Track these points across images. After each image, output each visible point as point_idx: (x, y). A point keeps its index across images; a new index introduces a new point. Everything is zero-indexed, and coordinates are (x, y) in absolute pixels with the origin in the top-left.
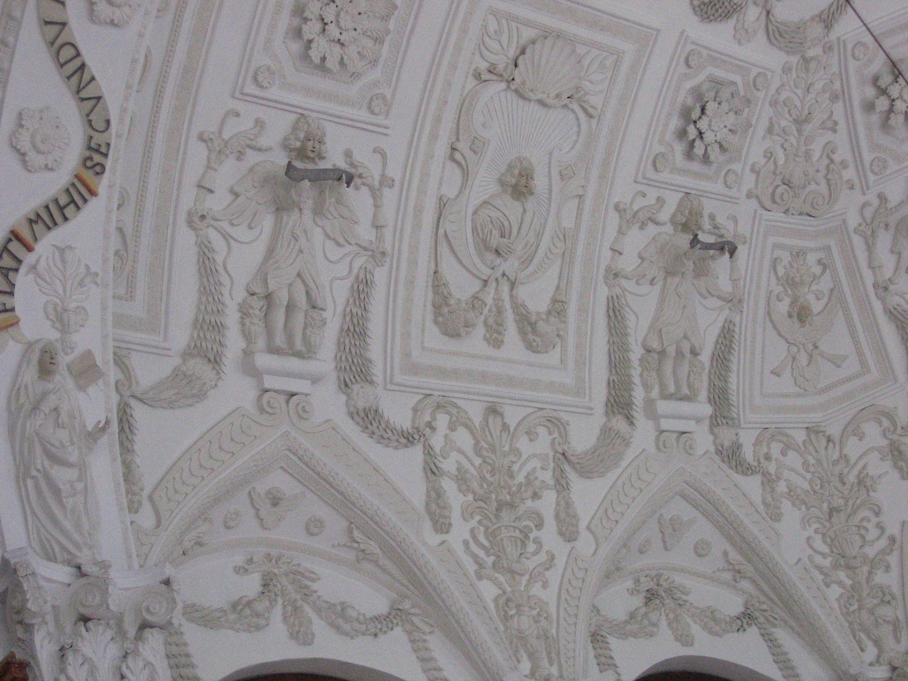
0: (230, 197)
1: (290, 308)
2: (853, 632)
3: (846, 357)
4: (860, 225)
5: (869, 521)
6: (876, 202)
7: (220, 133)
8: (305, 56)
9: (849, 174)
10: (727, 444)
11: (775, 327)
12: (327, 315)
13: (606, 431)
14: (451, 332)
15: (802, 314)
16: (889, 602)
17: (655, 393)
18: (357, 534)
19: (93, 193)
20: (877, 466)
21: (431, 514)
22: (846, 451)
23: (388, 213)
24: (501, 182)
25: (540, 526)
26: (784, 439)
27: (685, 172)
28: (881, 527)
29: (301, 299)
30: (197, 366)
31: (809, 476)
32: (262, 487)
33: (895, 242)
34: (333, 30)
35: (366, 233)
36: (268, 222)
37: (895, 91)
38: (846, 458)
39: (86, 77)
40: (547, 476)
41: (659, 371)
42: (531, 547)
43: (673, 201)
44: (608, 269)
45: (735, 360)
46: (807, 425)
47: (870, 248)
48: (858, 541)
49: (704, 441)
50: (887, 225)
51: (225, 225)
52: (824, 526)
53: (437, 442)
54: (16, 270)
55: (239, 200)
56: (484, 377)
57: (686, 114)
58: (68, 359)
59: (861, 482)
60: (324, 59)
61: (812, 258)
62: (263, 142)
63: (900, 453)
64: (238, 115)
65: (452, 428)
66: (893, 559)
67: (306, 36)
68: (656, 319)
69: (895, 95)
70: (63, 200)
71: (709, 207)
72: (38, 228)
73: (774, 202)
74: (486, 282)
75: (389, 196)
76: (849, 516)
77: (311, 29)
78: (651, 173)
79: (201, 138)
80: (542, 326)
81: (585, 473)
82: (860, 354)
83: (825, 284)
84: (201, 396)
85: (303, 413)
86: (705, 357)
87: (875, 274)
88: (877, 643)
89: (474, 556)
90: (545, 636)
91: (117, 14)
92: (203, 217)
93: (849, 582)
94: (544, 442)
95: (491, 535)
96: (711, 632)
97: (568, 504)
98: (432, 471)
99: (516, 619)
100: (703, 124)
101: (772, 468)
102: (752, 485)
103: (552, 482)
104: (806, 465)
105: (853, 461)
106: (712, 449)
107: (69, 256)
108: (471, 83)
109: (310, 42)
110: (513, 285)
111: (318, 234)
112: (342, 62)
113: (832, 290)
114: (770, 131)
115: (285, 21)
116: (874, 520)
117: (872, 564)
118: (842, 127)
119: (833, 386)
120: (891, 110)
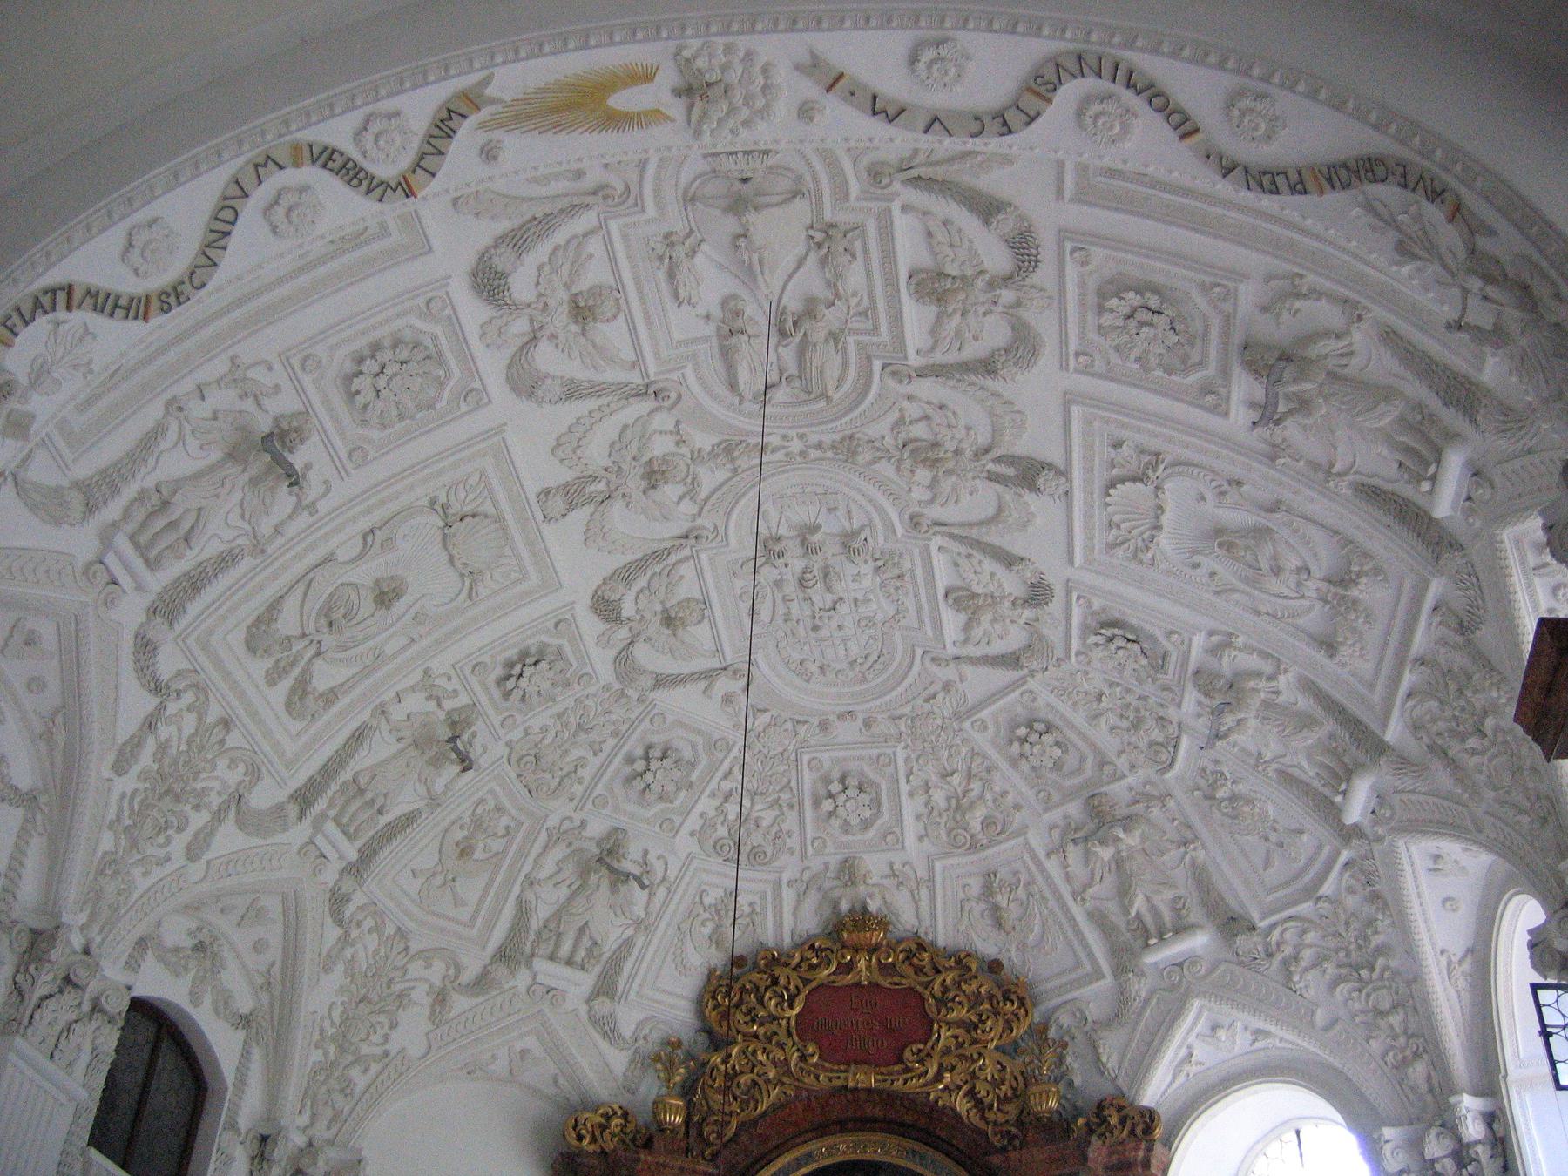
0: (209, 415)
1: (172, 525)
2: (306, 1093)
5: (382, 1027)
7: (249, 368)
8: (349, 378)
9: (578, 789)
10: (343, 890)
11: (441, 844)
12: (190, 554)
13: (280, 807)
14: (251, 646)
17: (332, 813)
18: (59, 720)
19: (145, 318)
20: (421, 995)
21: (121, 753)
23: (292, 529)
24: (377, 582)
25: (180, 830)
26: (379, 922)
27: (486, 689)
28: (386, 1038)
29: (185, 526)
30: (76, 500)
32: (31, 623)
33: (564, 859)
34: (382, 382)
35: (266, 528)
36: (216, 455)
37: (654, 765)
38: (406, 971)
39: (222, 243)
40: (215, 801)
41: (348, 802)
42: (161, 840)
43: (464, 699)
44: (382, 705)
45: (399, 840)
47: (546, 848)
48: (363, 1036)
49: (330, 875)
51: (188, 428)
53: (172, 708)
54: (46, 312)
55: (216, 424)
56: (242, 695)
57: (524, 654)
58: (18, 406)
59: (401, 995)
60: (358, 392)
61: (505, 821)
62: (266, 402)
63: (444, 999)
64: (270, 369)
65: (190, 709)
66: (375, 1068)
67: (364, 368)
68: (379, 765)
69: (653, 768)
70: (123, 302)
71: (479, 726)
72: (89, 301)
73: (518, 762)
74: (304, 635)
75: (304, 519)
77: (370, 366)
78: (467, 670)
79: (233, 359)
80: (310, 700)
81: (241, 824)
82: (478, 910)
83: (497, 845)
84: (58, 522)
85: (109, 602)
86: (384, 820)
88: (314, 1116)
89: (120, 809)
90: (115, 908)
91: (283, 227)
92: (180, 409)
93: (332, 1057)
94: (235, 776)
95: (145, 805)
96: (216, 1011)
97: (212, 834)
98: (150, 724)
99: (108, 878)
100: (528, 671)
101: (354, 934)
102: (333, 933)
103: (215, 808)
104: (376, 952)
105: (408, 977)
106: (331, 885)
107: (89, 338)
108: (425, 501)
109: (361, 373)
110: (318, 654)
111: (237, 496)
112: (365, 407)
113: (497, 853)
114: (560, 716)
115: (361, 344)
117: (358, 1060)
118: (602, 756)
120: (641, 775)
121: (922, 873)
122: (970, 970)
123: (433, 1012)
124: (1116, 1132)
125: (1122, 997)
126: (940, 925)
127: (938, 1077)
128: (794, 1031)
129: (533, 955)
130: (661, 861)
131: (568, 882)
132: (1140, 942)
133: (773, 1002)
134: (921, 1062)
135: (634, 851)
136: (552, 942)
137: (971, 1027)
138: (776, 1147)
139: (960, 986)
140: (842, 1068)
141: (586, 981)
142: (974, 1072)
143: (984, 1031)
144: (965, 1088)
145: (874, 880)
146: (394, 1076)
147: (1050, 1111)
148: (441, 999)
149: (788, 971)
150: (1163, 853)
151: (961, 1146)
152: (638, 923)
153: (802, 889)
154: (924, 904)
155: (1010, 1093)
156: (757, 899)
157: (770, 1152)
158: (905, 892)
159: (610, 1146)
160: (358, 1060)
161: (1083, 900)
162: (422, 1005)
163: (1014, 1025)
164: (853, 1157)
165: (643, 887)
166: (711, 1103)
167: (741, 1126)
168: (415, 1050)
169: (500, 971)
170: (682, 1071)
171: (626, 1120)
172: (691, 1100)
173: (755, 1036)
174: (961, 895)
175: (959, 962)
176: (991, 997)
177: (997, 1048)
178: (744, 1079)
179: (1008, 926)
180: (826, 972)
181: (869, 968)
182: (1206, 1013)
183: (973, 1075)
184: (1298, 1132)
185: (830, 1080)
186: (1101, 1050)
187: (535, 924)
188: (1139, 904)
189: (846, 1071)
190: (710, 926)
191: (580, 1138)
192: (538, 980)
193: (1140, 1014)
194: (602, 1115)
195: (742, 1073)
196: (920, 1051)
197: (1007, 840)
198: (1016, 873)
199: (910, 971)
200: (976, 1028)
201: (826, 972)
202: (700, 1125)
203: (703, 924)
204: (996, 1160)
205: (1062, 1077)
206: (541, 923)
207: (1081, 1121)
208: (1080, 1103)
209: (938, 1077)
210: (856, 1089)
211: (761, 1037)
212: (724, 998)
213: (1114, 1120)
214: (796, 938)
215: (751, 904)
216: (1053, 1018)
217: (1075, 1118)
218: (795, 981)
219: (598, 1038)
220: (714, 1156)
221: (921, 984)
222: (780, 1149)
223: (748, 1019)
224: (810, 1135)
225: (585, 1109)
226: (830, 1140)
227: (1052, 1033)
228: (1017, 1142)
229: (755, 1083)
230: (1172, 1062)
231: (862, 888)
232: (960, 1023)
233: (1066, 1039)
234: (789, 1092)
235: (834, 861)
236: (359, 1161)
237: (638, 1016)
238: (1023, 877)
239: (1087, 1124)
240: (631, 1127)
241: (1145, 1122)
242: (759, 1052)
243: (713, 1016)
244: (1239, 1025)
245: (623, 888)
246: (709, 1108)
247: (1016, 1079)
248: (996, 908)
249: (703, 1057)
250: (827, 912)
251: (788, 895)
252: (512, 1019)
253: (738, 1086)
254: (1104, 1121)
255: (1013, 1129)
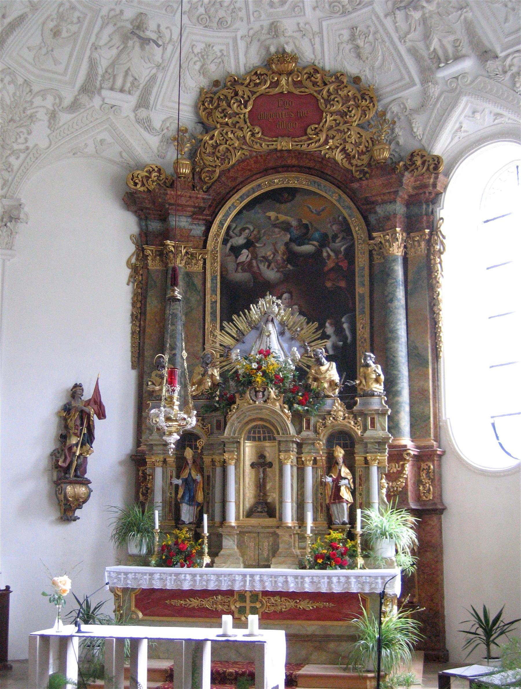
3: (60, 63)
4: (105, 16)
5: (23, 134)
6: (118, 12)
15: (56, 33)
16: (9, 172)
20: (42, 115)
22: (34, 100)
28: (26, 140)
31: (13, 99)
38: (32, 103)
46: (26, 79)
47: (102, 28)
50: (115, 24)
52: (4, 124)
59: (31, 117)
61: (77, 14)
63: (55, 116)
76: (17, 127)
83: (74, 28)
86: (7, 21)
87: (96, 40)
104: (14, 94)
105: (34, 106)
113: (75, 33)
116: (26, 135)
117: (13, 152)
119: (48, 71)
121: (316, 28)
122: (343, 83)
123: (50, 123)
124: (419, 169)
125: (425, 95)
126: (326, 57)
127: (326, 142)
128: (248, 120)
129: (101, 88)
130: (168, 30)
131: (117, 45)
132: (434, 67)
133: (235, 105)
134: (317, 134)
135: (152, 25)
136: (111, 80)
137: (343, 114)
138: (242, 182)
139: (338, 92)
140: (274, 139)
141: (133, 100)
142: (345, 138)
143: (350, 116)
144: (341, 147)
145: (289, 33)
146: (33, 160)
147: (385, 159)
148: (53, 116)
149: (243, 88)
150: (449, 15)
151: (339, 179)
152: (158, 66)
153: (249, 40)
154: (318, 47)
155: (364, 150)
156: (224, 47)
157: (239, 185)
158: (306, 40)
159: (152, 187)
160: (13, 152)
161: (405, 42)
162: (43, 121)
163: (367, 112)
164: (283, 186)
165: (158, 46)
166: (206, 162)
167: (222, 173)
168: (43, 144)
169: (84, 99)
170: (188, 145)
171: (160, 174)
172: (194, 160)
173: (227, 124)
174: (338, 41)
175: (337, 78)
176: (354, 98)
177: (358, 125)
178: (221, 148)
179: (364, 58)
180: (264, 87)
181: (287, 83)
182: (469, 105)
183: (345, 141)
184: (517, 167)
185: (268, 146)
186: (413, 125)
187: (100, 71)
188: (435, 44)
189: (276, 141)
190: (199, 64)
191: (136, 184)
192: (106, 101)
193: (435, 105)
194: (147, 172)
195: (221, 144)
196: (316, 128)
197: (361, 9)
198: (368, 27)
199: (310, 84)
200: (346, 115)
201: (264, 87)
202: (200, 173)
203: (195, 63)
204: (355, 185)
205: (393, 140)
206: (104, 71)
207: (401, 164)
208: (402, 154)
209: (326, 142)
210: (281, 151)
211: (230, 125)
212: (209, 104)
213: (419, 163)
214: (247, 68)
215: (221, 51)
216: (389, 108)
217: (399, 162)
218: (248, 93)
219: (142, 130)
220: (208, 189)
221: (316, 91)
222: (243, 183)
223: (222, 115)
224: (258, 176)
225: (137, 169)
226: (269, 177)
227: (388, 116)
228: (367, 175)
229: (228, 149)
230: (450, 131)
231: (282, 40)
232: (338, 113)
233: (396, 119)
234: (246, 154)
235: (266, 24)
236: (20, 205)
237: (164, 117)
238: (372, 29)
239: (405, 165)
240: (163, 177)
241: (435, 164)
242: (229, 133)
243: (203, 114)
244: (487, 111)
245: (147, 47)
246: (204, 164)
247: (368, 142)
248: (357, 47)
249: (199, 137)
250: (264, 52)
251: (242, 45)
252: (91, 125)
253: (219, 152)
254: (414, 163)
255: (366, 169)
